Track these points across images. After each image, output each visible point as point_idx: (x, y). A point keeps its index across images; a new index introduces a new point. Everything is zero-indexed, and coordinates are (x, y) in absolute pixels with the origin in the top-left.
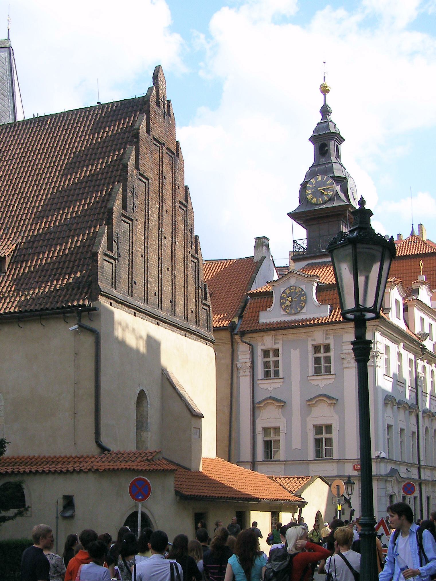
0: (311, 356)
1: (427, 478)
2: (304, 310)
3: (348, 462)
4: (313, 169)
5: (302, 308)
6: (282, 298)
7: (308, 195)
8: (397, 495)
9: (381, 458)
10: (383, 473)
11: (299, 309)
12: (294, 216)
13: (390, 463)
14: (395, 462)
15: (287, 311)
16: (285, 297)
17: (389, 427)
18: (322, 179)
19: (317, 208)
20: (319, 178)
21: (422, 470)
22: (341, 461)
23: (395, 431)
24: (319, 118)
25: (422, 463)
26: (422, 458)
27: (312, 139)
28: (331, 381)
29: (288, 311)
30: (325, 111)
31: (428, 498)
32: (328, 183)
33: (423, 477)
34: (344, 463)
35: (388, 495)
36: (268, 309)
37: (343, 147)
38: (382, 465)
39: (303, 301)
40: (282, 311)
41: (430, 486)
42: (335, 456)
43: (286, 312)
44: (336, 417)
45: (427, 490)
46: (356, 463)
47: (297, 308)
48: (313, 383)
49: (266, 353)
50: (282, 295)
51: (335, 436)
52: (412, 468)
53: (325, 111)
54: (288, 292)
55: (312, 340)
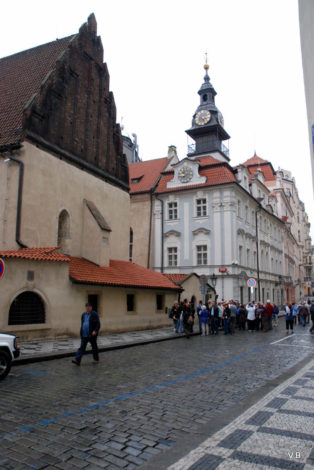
0: (195, 206)
1: (263, 278)
2: (192, 180)
3: (215, 267)
4: (200, 107)
5: (190, 179)
6: (179, 174)
7: (196, 121)
8: (245, 286)
9: (235, 265)
10: (236, 274)
11: (189, 180)
12: (189, 132)
13: (241, 268)
14: (243, 268)
17: (241, 247)
18: (204, 112)
19: (201, 127)
20: (202, 111)
21: (260, 274)
22: (212, 267)
23: (244, 250)
24: (203, 82)
25: (260, 269)
26: (259, 267)
27: (200, 93)
28: (206, 220)
30: (207, 79)
31: (263, 289)
32: (207, 114)
33: (260, 278)
34: (214, 267)
35: (240, 286)
36: (172, 180)
37: (216, 97)
38: (236, 269)
39: (191, 175)
40: (179, 181)
41: (264, 282)
42: (209, 263)
44: (209, 241)
45: (263, 285)
46: (221, 268)
47: (187, 179)
48: (196, 221)
49: (170, 205)
51: (208, 252)
52: (254, 272)
53: (207, 79)
54: (183, 170)
55: (196, 197)
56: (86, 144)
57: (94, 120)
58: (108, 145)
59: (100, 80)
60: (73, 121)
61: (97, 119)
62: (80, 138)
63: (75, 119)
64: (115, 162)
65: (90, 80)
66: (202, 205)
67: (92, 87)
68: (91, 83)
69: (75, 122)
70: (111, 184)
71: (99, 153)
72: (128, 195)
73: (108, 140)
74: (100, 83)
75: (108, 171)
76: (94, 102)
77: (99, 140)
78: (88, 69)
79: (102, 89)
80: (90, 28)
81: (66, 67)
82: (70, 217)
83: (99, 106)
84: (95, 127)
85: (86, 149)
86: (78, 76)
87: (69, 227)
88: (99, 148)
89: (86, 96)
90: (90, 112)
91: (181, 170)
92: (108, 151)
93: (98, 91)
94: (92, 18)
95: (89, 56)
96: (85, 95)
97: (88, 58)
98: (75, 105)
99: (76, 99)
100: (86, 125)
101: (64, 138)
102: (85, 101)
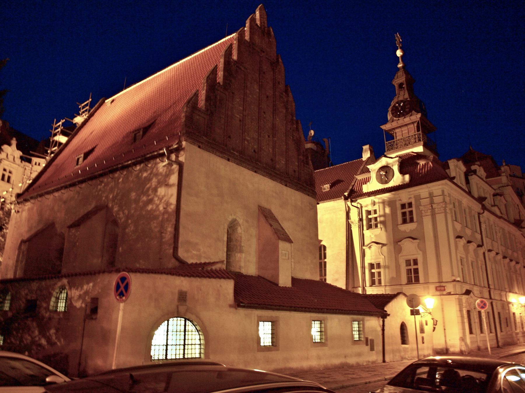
58: (287, 144)
59: (273, 73)
62: (251, 137)
63: (245, 116)
64: (297, 163)
66: (407, 210)
67: (263, 81)
71: (275, 154)
74: (273, 76)
76: (267, 97)
83: (273, 101)
84: (269, 125)
87: (241, 239)
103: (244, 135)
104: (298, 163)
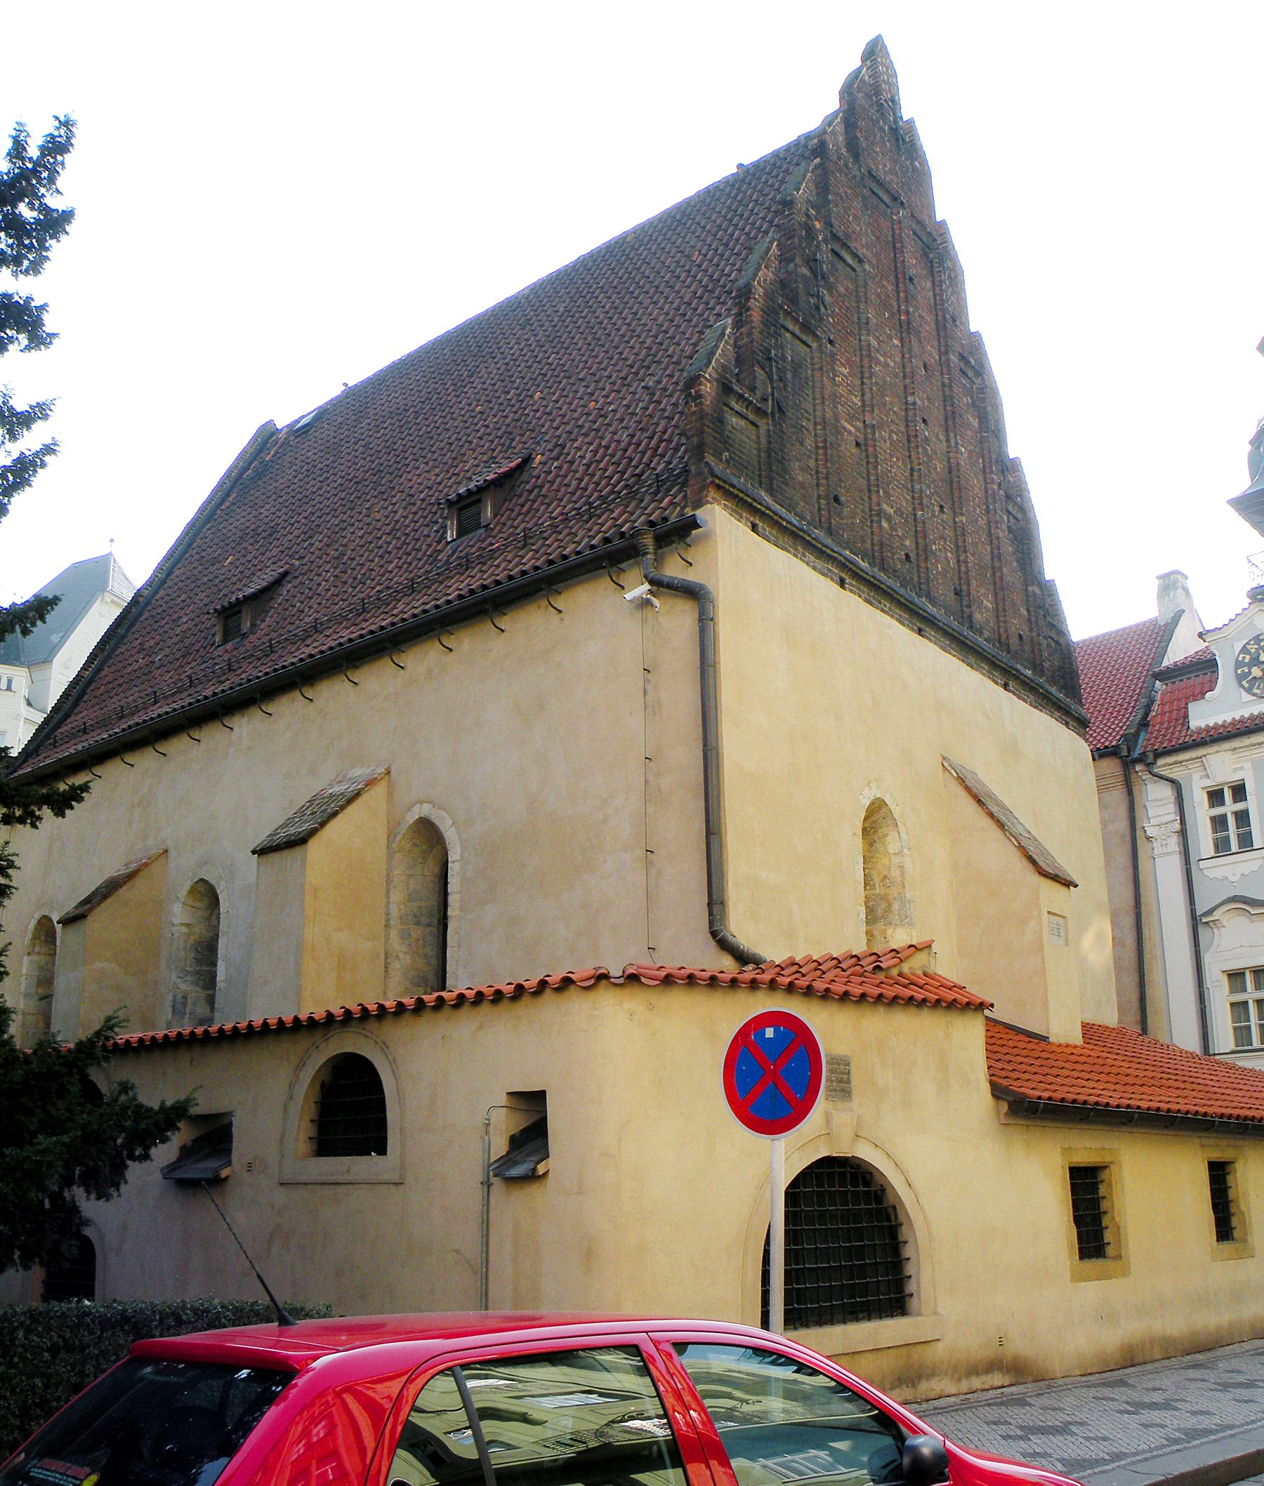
6: (1238, 664)
15: (1255, 691)
16: (1247, 660)
29: (1258, 692)
40: (1243, 693)
43: (1254, 695)
50: (1240, 659)
56: (920, 535)
57: (932, 433)
60: (866, 439)
61: (942, 437)
65: (901, 278)
68: (906, 292)
69: (874, 440)
70: (1025, 701)
71: (967, 572)
72: (1084, 749)
73: (989, 522)
74: (935, 296)
75: (1008, 645)
77: (964, 519)
78: (890, 239)
79: (944, 315)
80: (876, 90)
81: (818, 225)
82: (902, 829)
83: (943, 385)
85: (924, 552)
86: (861, 261)
87: (902, 874)
88: (965, 551)
89: (896, 342)
90: (919, 402)
91: (1244, 650)
92: (997, 564)
93: (933, 326)
94: (874, 53)
95: (888, 192)
96: (890, 337)
97: (885, 198)
98: (862, 374)
99: (865, 353)
100: (910, 457)
101: (843, 499)
102: (895, 362)
103: (874, 500)
104: (1028, 610)
